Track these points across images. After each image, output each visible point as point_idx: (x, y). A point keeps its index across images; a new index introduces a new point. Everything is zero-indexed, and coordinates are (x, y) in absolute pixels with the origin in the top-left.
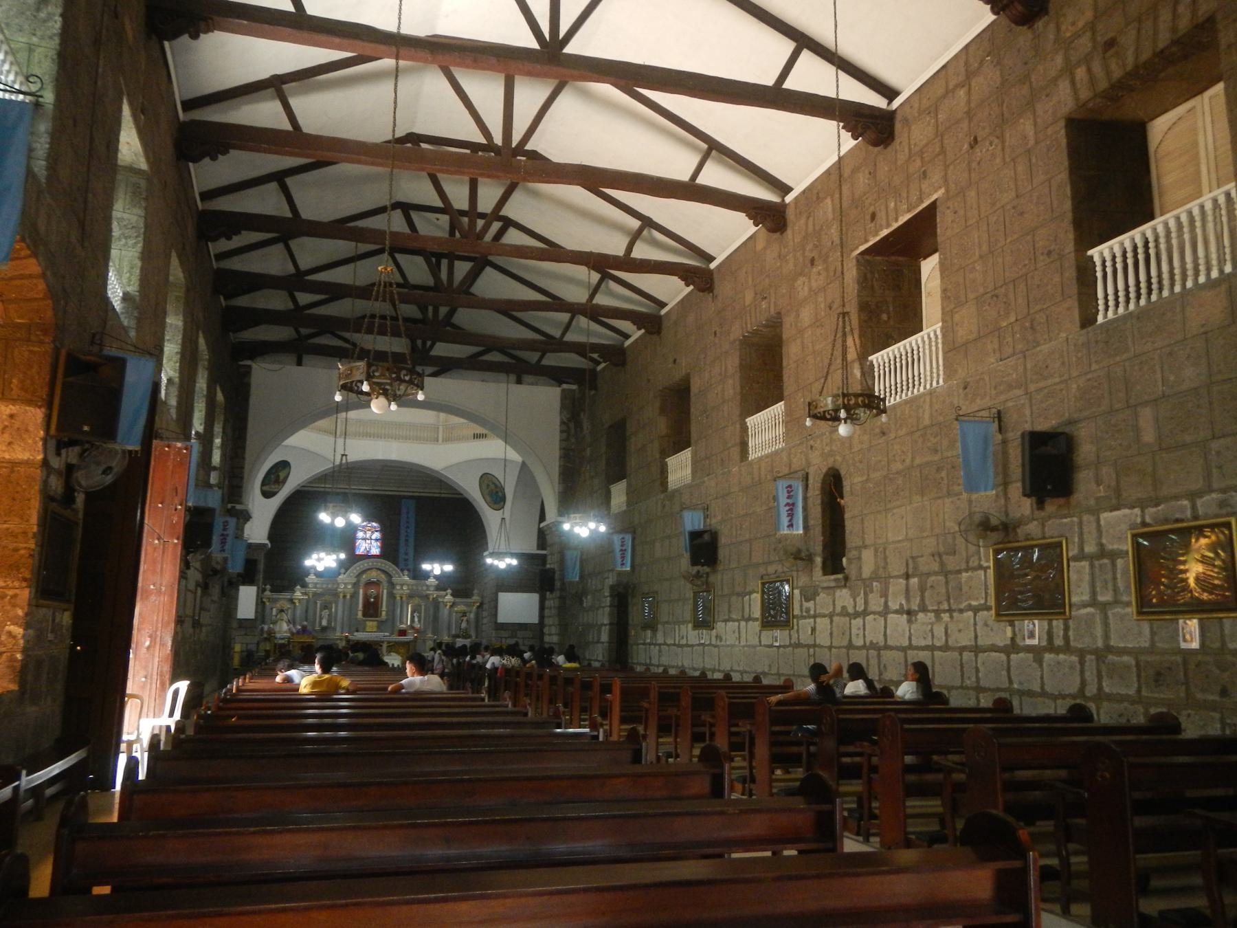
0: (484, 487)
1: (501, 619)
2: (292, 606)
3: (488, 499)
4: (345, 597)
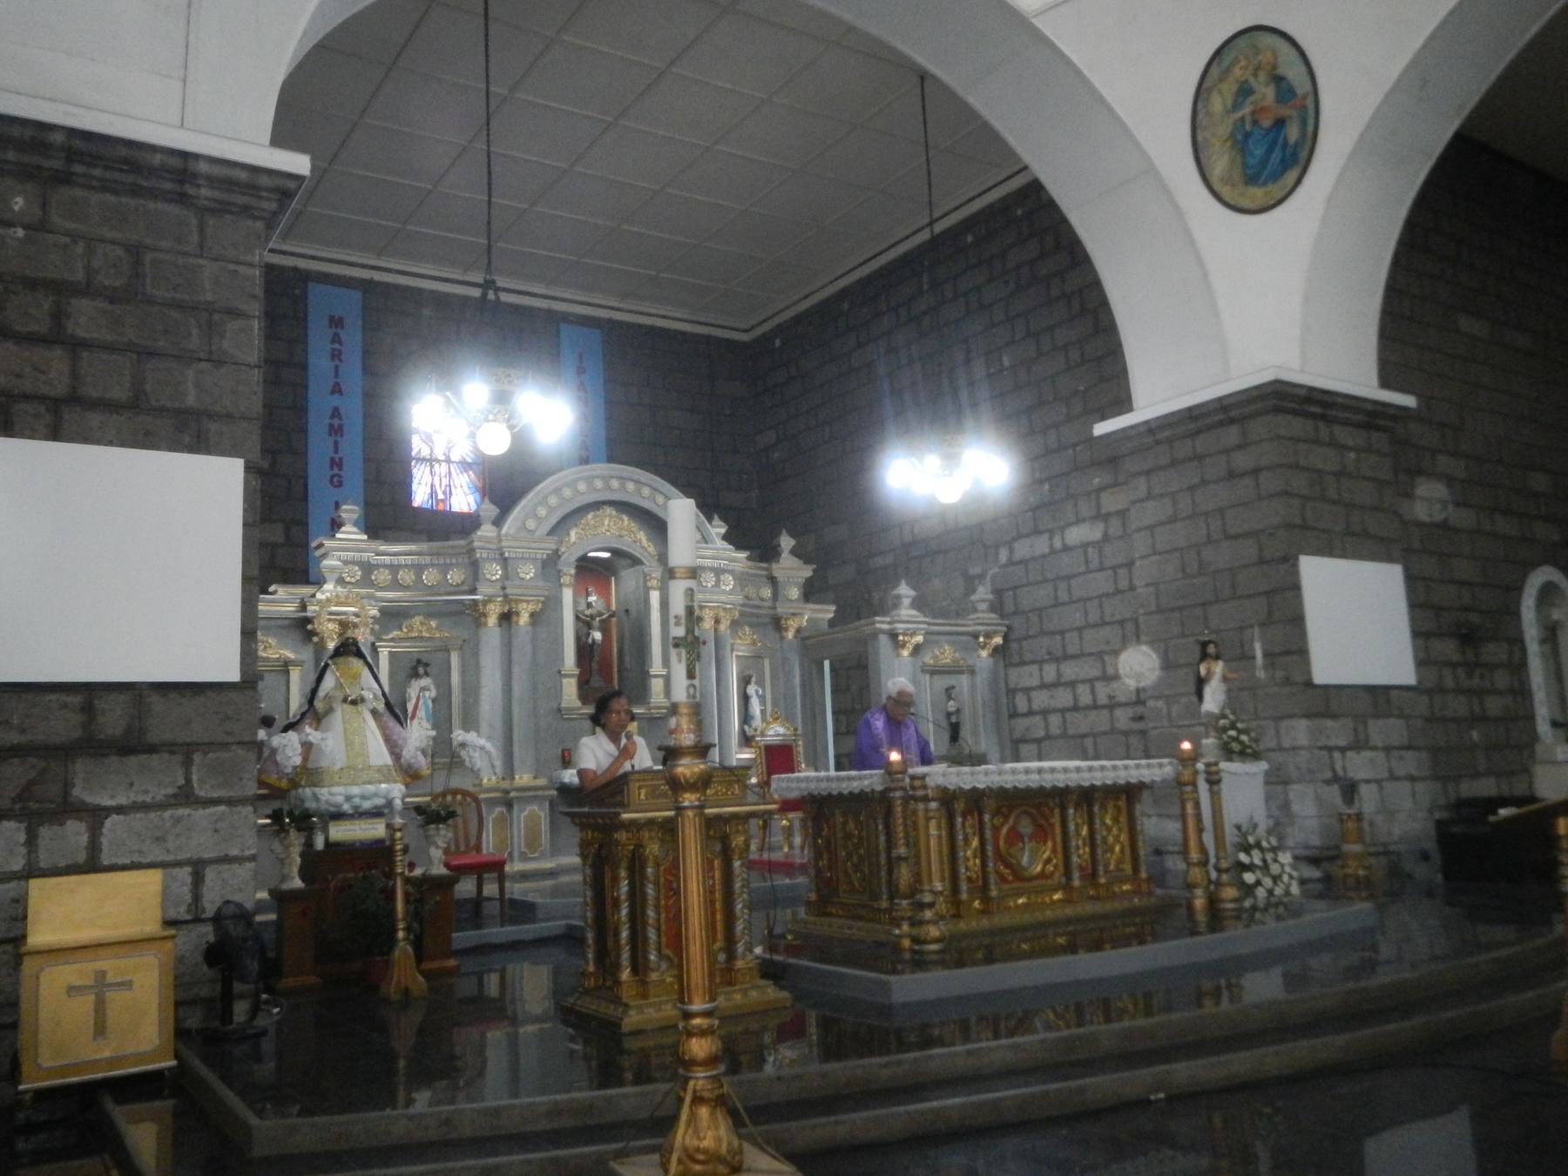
0: (1217, 104)
1: (1320, 677)
2: (307, 654)
3: (1220, 164)
4: (506, 618)
